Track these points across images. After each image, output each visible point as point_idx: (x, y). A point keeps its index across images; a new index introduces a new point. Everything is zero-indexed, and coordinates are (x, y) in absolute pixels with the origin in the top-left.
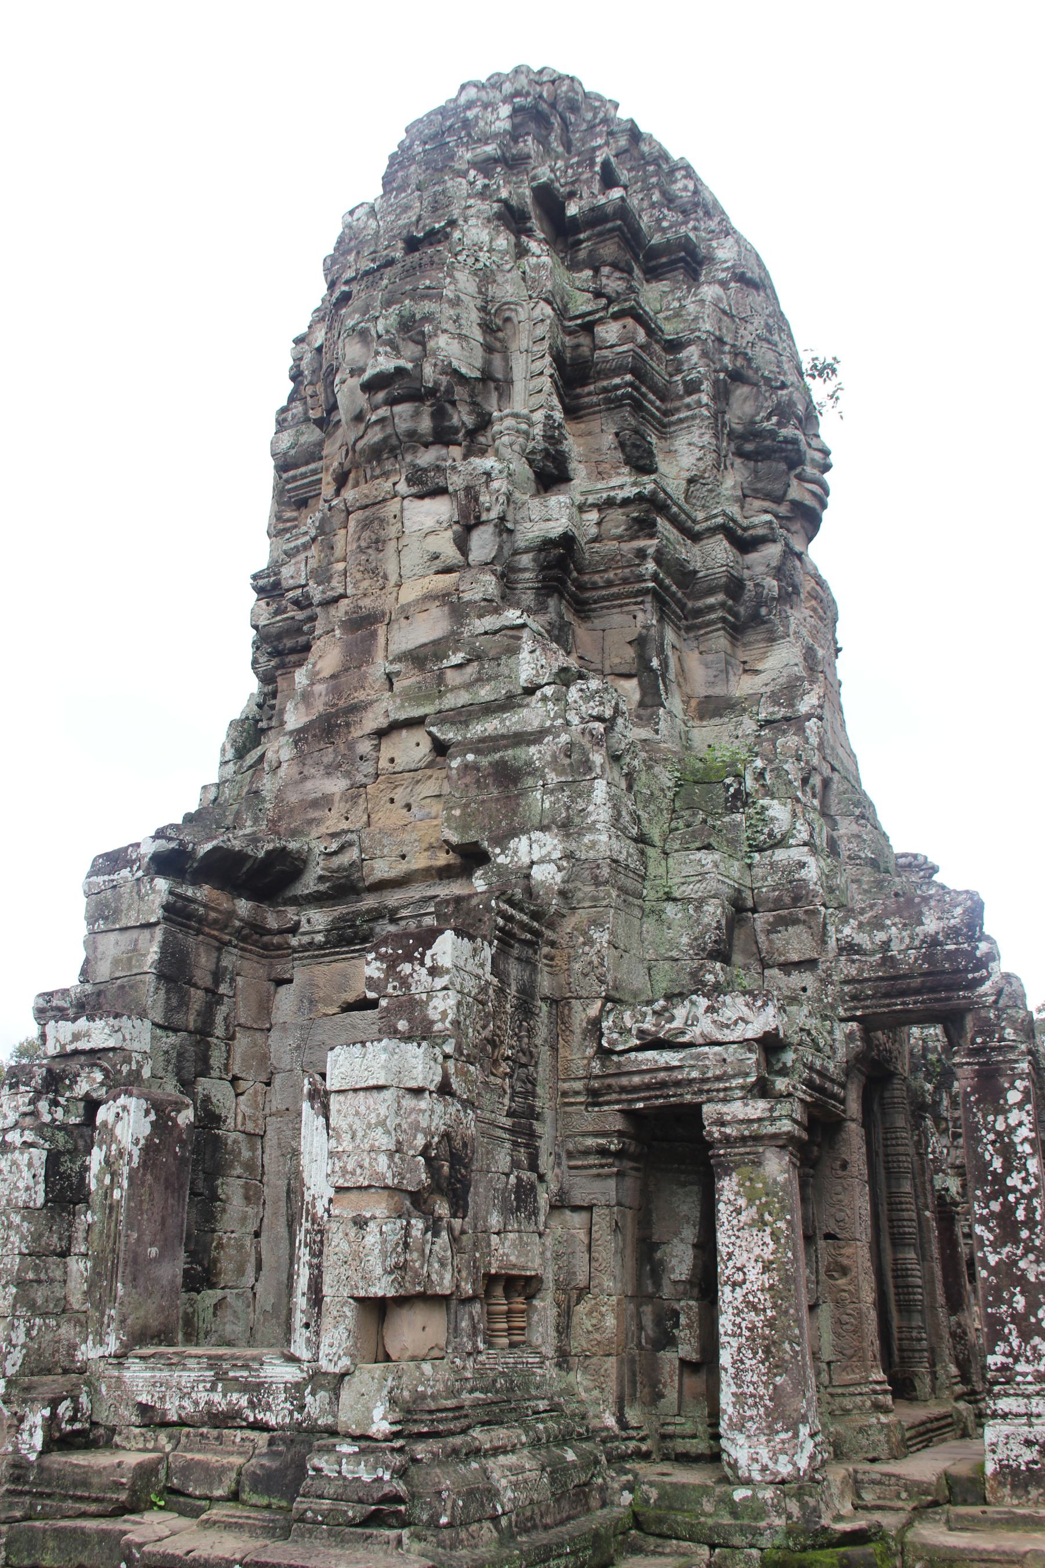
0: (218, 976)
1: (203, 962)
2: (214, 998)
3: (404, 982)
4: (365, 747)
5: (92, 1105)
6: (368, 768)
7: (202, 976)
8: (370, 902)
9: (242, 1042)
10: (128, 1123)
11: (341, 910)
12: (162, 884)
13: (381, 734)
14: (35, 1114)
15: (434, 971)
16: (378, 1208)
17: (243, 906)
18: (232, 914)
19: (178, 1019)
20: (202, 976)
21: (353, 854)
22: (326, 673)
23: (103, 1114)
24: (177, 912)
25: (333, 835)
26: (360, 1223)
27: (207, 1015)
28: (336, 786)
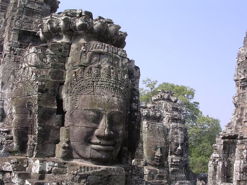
0: (229, 148)
1: (228, 147)
2: (229, 150)
3: (242, 153)
4: (243, 123)
5: (217, 162)
6: (243, 125)
7: (228, 148)
8: (244, 140)
9: (232, 154)
10: (220, 164)
11: (242, 140)
12: (223, 140)
13: (245, 122)
14: (213, 163)
15: (244, 153)
16: (238, 173)
17: (232, 140)
18: (230, 141)
19: (225, 153)
20: (228, 148)
21: (242, 135)
22: (239, 114)
23: (218, 163)
24: (224, 143)
25: (240, 133)
26: (237, 174)
27: (228, 152)
28: (241, 127)
